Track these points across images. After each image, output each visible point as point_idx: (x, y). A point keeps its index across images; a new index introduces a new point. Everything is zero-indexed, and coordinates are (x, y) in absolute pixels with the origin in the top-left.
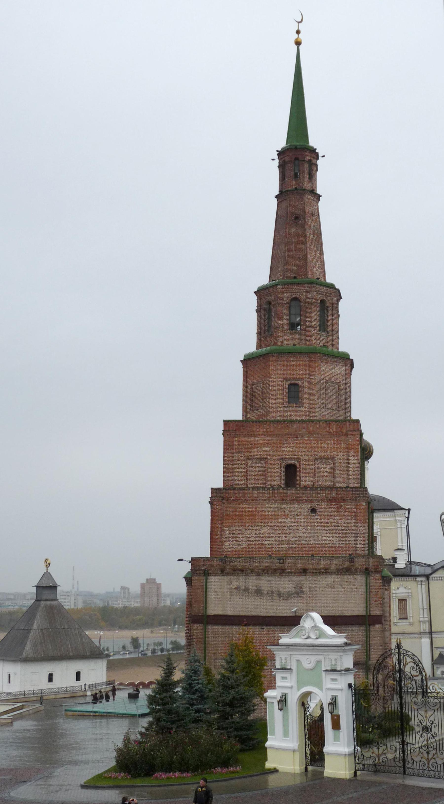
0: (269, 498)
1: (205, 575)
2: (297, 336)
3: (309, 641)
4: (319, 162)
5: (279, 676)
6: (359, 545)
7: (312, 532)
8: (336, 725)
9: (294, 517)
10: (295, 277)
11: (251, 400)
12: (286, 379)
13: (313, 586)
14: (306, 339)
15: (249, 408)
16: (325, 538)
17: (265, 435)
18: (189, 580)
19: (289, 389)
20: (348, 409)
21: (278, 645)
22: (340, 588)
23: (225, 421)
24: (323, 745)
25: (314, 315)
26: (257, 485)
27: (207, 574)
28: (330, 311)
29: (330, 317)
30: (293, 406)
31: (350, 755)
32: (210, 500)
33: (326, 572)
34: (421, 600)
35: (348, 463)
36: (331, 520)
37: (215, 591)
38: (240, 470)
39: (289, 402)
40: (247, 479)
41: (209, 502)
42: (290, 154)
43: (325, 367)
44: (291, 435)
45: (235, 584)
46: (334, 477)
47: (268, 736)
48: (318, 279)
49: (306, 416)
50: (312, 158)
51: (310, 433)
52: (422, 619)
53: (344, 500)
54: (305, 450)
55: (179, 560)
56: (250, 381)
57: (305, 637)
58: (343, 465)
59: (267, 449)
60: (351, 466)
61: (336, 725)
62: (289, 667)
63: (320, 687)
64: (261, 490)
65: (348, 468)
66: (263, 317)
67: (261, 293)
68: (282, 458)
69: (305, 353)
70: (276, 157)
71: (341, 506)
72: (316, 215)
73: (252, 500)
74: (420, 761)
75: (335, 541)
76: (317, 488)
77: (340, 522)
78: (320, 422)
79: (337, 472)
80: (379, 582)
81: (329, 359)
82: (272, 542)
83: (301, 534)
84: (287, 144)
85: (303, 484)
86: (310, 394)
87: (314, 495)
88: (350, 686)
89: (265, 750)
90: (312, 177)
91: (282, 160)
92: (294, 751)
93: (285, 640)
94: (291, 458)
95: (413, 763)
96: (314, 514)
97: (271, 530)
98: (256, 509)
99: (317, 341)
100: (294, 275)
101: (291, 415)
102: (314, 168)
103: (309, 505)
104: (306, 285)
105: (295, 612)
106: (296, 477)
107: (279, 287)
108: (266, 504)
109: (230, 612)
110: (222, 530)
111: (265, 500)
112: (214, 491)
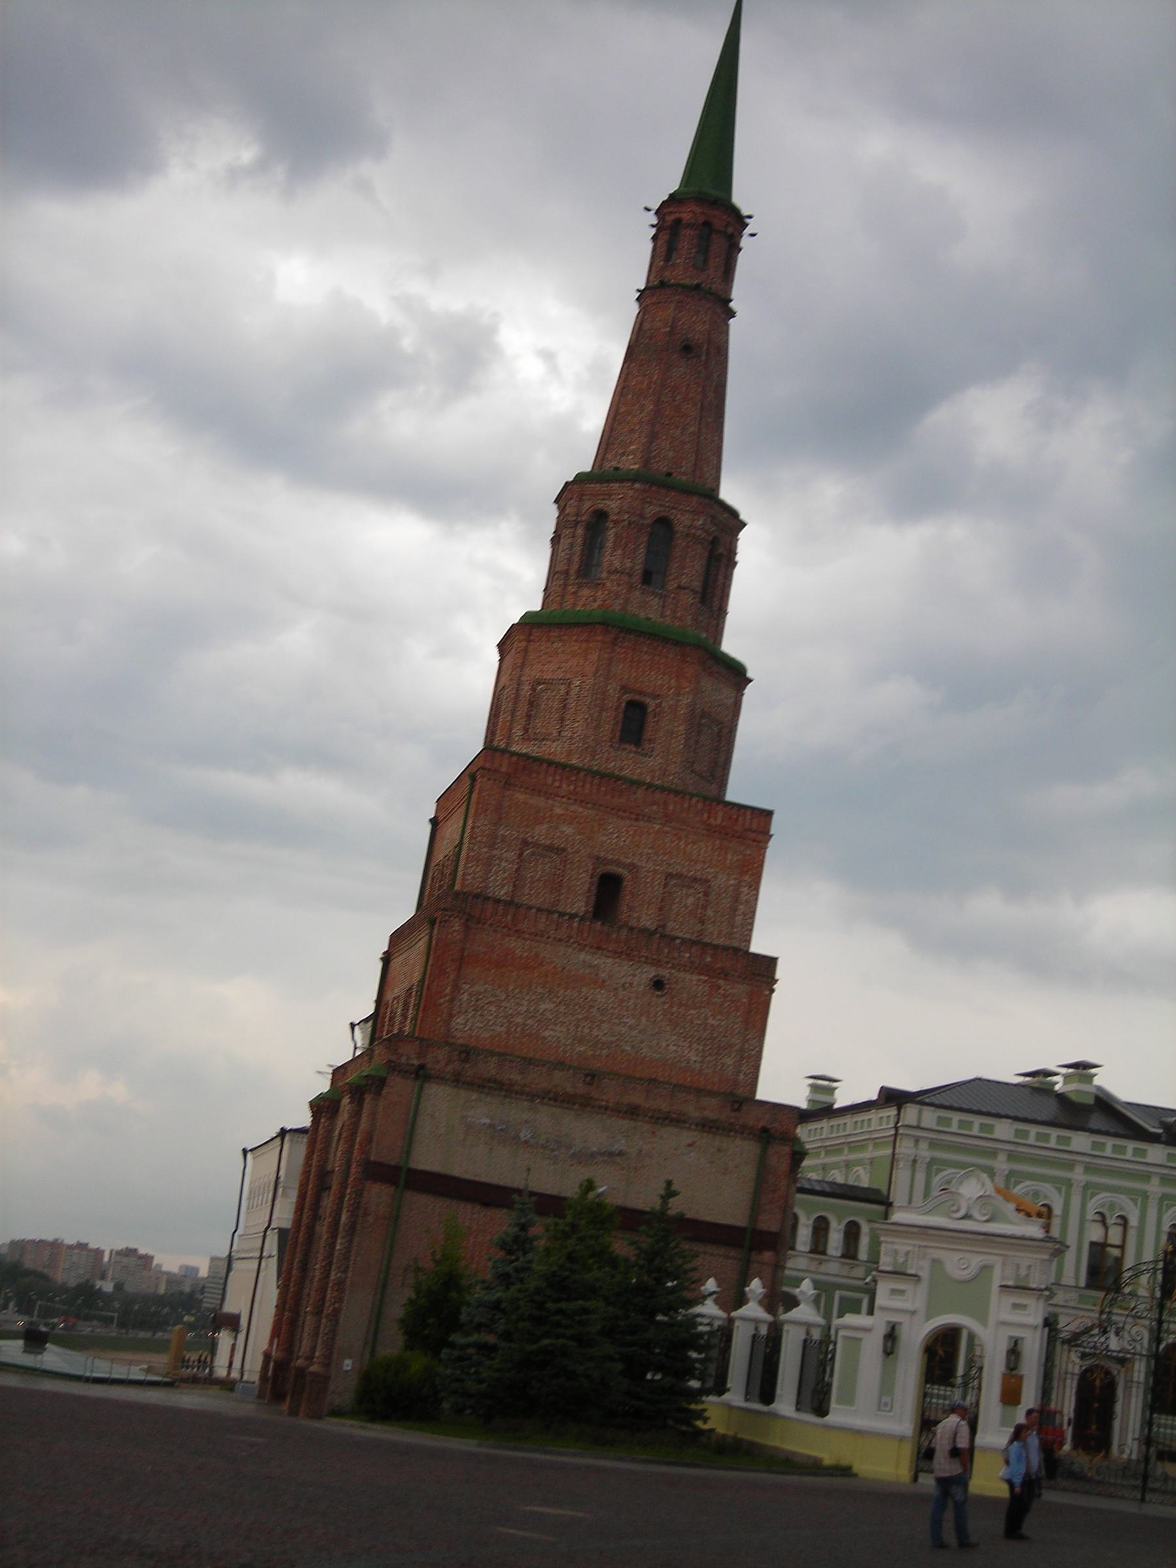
0: (570, 937)
1: (417, 1077)
6: (741, 1077)
10: (669, 474)
11: (529, 716)
14: (674, 612)
15: (518, 732)
19: (626, 711)
27: (421, 1074)
30: (630, 752)
33: (676, 1120)
35: (736, 899)
36: (692, 1012)
38: (503, 864)
39: (622, 740)
40: (515, 886)
42: (698, 210)
43: (707, 684)
49: (653, 777)
56: (532, 673)
57: (960, 1215)
59: (568, 830)
62: (912, 1272)
63: (983, 1318)
64: (556, 916)
65: (734, 910)
66: (580, 541)
68: (598, 858)
69: (677, 643)
71: (719, 987)
73: (531, 934)
79: (710, 913)
83: (624, 1030)
85: (633, 923)
87: (666, 950)
91: (673, 217)
92: (902, 1439)
94: (618, 863)
97: (562, 1009)
98: (537, 955)
101: (621, 769)
104: (695, 499)
107: (637, 486)
109: (461, 1168)
110: (456, 988)
111: (560, 940)
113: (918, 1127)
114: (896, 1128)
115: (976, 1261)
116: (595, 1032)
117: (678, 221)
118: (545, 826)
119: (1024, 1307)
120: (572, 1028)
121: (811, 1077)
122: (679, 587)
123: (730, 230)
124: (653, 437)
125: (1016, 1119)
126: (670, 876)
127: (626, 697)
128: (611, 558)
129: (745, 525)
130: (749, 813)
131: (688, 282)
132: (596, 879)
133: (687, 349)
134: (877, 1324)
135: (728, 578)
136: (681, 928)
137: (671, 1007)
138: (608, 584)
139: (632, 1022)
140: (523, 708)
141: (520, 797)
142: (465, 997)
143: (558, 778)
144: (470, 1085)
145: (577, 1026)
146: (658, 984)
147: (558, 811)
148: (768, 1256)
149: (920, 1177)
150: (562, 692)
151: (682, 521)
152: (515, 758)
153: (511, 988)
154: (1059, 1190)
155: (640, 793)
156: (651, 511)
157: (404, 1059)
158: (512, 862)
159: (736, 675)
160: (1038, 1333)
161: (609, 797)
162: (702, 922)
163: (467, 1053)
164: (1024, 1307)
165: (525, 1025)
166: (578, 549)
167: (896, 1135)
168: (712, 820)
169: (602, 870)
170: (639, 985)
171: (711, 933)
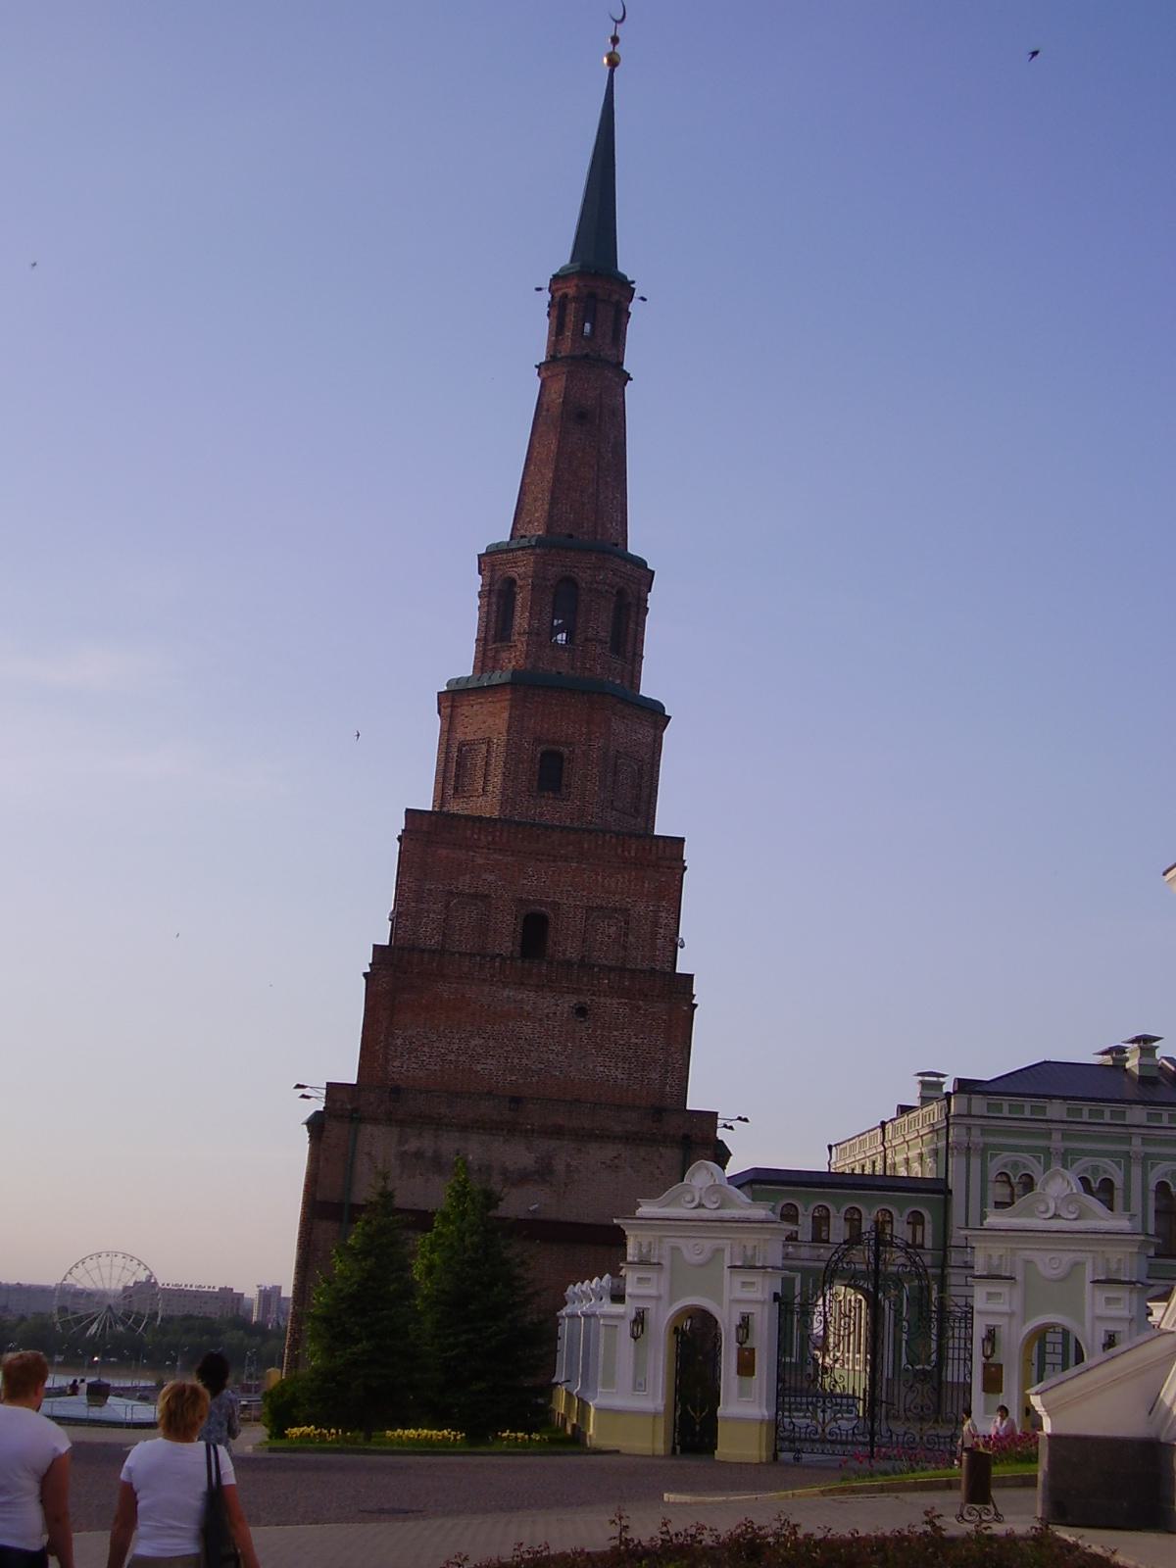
0: (492, 976)
3: (703, 1213)
8: (746, 1367)
9: (541, 1020)
13: (574, 1163)
16: (602, 1069)
17: (489, 849)
19: (541, 761)
30: (549, 798)
32: (368, 970)
33: (602, 1137)
35: (656, 924)
36: (615, 1033)
37: (369, 1154)
40: (444, 934)
44: (543, 855)
45: (412, 1145)
48: (617, 545)
50: (622, 299)
53: (646, 996)
54: (570, 889)
56: (459, 736)
57: (693, 1205)
58: (645, 927)
59: (491, 878)
60: (661, 931)
61: (746, 1367)
62: (655, 1261)
65: (654, 935)
66: (494, 607)
67: (491, 560)
68: (520, 899)
70: (546, 284)
74: (906, 1433)
75: (620, 1076)
76: (594, 966)
77: (633, 1040)
78: (604, 835)
82: (492, 1067)
84: (572, 261)
91: (560, 293)
92: (655, 1415)
93: (646, 1209)
95: (891, 1436)
96: (582, 1019)
97: (491, 1043)
98: (463, 996)
100: (567, 532)
101: (542, 814)
103: (573, 1000)
105: (534, 1211)
107: (538, 551)
113: (970, 1116)
114: (947, 1118)
115: (708, 1245)
117: (565, 296)
118: (468, 876)
120: (502, 1060)
121: (919, 1074)
122: (586, 640)
123: (615, 297)
125: (1065, 1098)
126: (591, 908)
127: (542, 748)
128: (521, 621)
129: (653, 572)
130: (661, 841)
133: (582, 416)
134: (627, 1309)
135: (641, 624)
137: (594, 1031)
138: (519, 646)
139: (557, 1048)
141: (443, 852)
142: (399, 1042)
143: (477, 831)
145: (506, 1058)
146: (581, 1011)
147: (480, 861)
149: (976, 1162)
150: (484, 751)
152: (433, 818)
153: (442, 1028)
154: (1118, 1164)
157: (338, 1104)
158: (439, 914)
159: (656, 716)
161: (525, 843)
162: (625, 948)
163: (396, 1091)
165: (457, 1061)
167: (948, 1124)
168: (626, 853)
170: (562, 1014)
171: (636, 958)
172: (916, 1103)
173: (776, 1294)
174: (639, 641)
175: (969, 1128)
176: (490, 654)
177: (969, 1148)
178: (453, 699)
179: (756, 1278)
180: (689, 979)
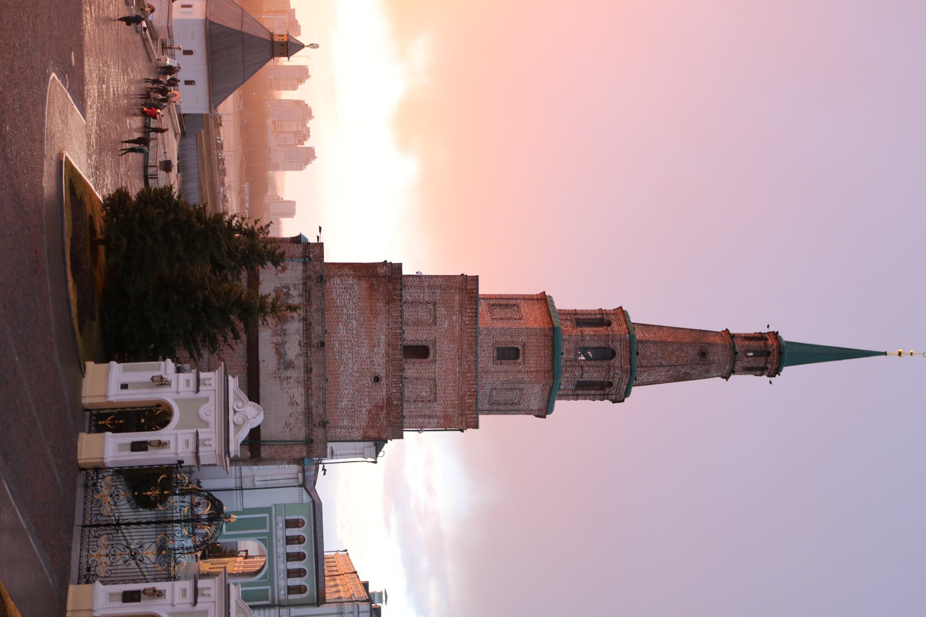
2: (572, 356)
4: (764, 377)
5: (190, 376)
7: (352, 379)
10: (638, 354)
11: (500, 305)
12: (524, 345)
13: (292, 381)
15: (492, 302)
18: (298, 240)
20: (489, 412)
21: (226, 375)
22: (290, 411)
23: (477, 277)
24: (114, 431)
25: (595, 375)
26: (406, 315)
28: (599, 392)
29: (593, 392)
31: (103, 463)
33: (308, 395)
34: (278, 477)
35: (430, 417)
39: (498, 349)
41: (385, 261)
42: (774, 347)
43: (537, 388)
45: (293, 292)
46: (415, 402)
47: (122, 364)
51: (463, 374)
52: (256, 478)
55: (320, 228)
56: (522, 303)
59: (446, 324)
62: (201, 388)
63: (178, 427)
65: (424, 416)
66: (593, 317)
67: (621, 313)
69: (553, 367)
70: (771, 330)
72: (705, 375)
79: (420, 405)
80: (296, 455)
81: (546, 393)
83: (351, 365)
84: (786, 342)
85: (406, 366)
86: (507, 372)
88: (181, 462)
89: (107, 360)
90: (748, 370)
92: (106, 396)
93: (233, 382)
94: (435, 353)
97: (355, 332)
99: (566, 380)
102: (758, 373)
106: (414, 358)
108: (384, 326)
112: (399, 266)
116: (346, 351)
117: (767, 339)
119: (187, 445)
123: (769, 366)
124: (655, 343)
127: (520, 347)
128: (588, 331)
131: (737, 349)
132: (424, 343)
133: (703, 354)
136: (409, 391)
140: (505, 302)
141: (457, 298)
144: (305, 284)
146: (377, 379)
147: (454, 318)
148: (249, 454)
151: (616, 362)
155: (472, 357)
156: (617, 346)
159: (544, 411)
160: (174, 456)
162: (415, 402)
164: (187, 445)
166: (589, 317)
169: (430, 346)
172: (371, 590)
173: (183, 462)
174: (585, 397)
175: (352, 613)
176: (569, 317)
177: (342, 613)
178: (544, 300)
179: (192, 447)
180: (401, 437)
